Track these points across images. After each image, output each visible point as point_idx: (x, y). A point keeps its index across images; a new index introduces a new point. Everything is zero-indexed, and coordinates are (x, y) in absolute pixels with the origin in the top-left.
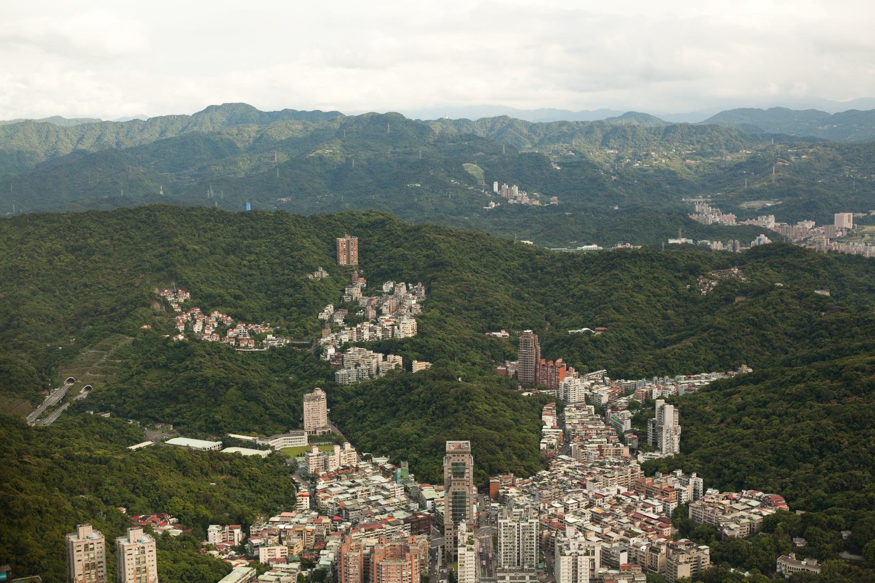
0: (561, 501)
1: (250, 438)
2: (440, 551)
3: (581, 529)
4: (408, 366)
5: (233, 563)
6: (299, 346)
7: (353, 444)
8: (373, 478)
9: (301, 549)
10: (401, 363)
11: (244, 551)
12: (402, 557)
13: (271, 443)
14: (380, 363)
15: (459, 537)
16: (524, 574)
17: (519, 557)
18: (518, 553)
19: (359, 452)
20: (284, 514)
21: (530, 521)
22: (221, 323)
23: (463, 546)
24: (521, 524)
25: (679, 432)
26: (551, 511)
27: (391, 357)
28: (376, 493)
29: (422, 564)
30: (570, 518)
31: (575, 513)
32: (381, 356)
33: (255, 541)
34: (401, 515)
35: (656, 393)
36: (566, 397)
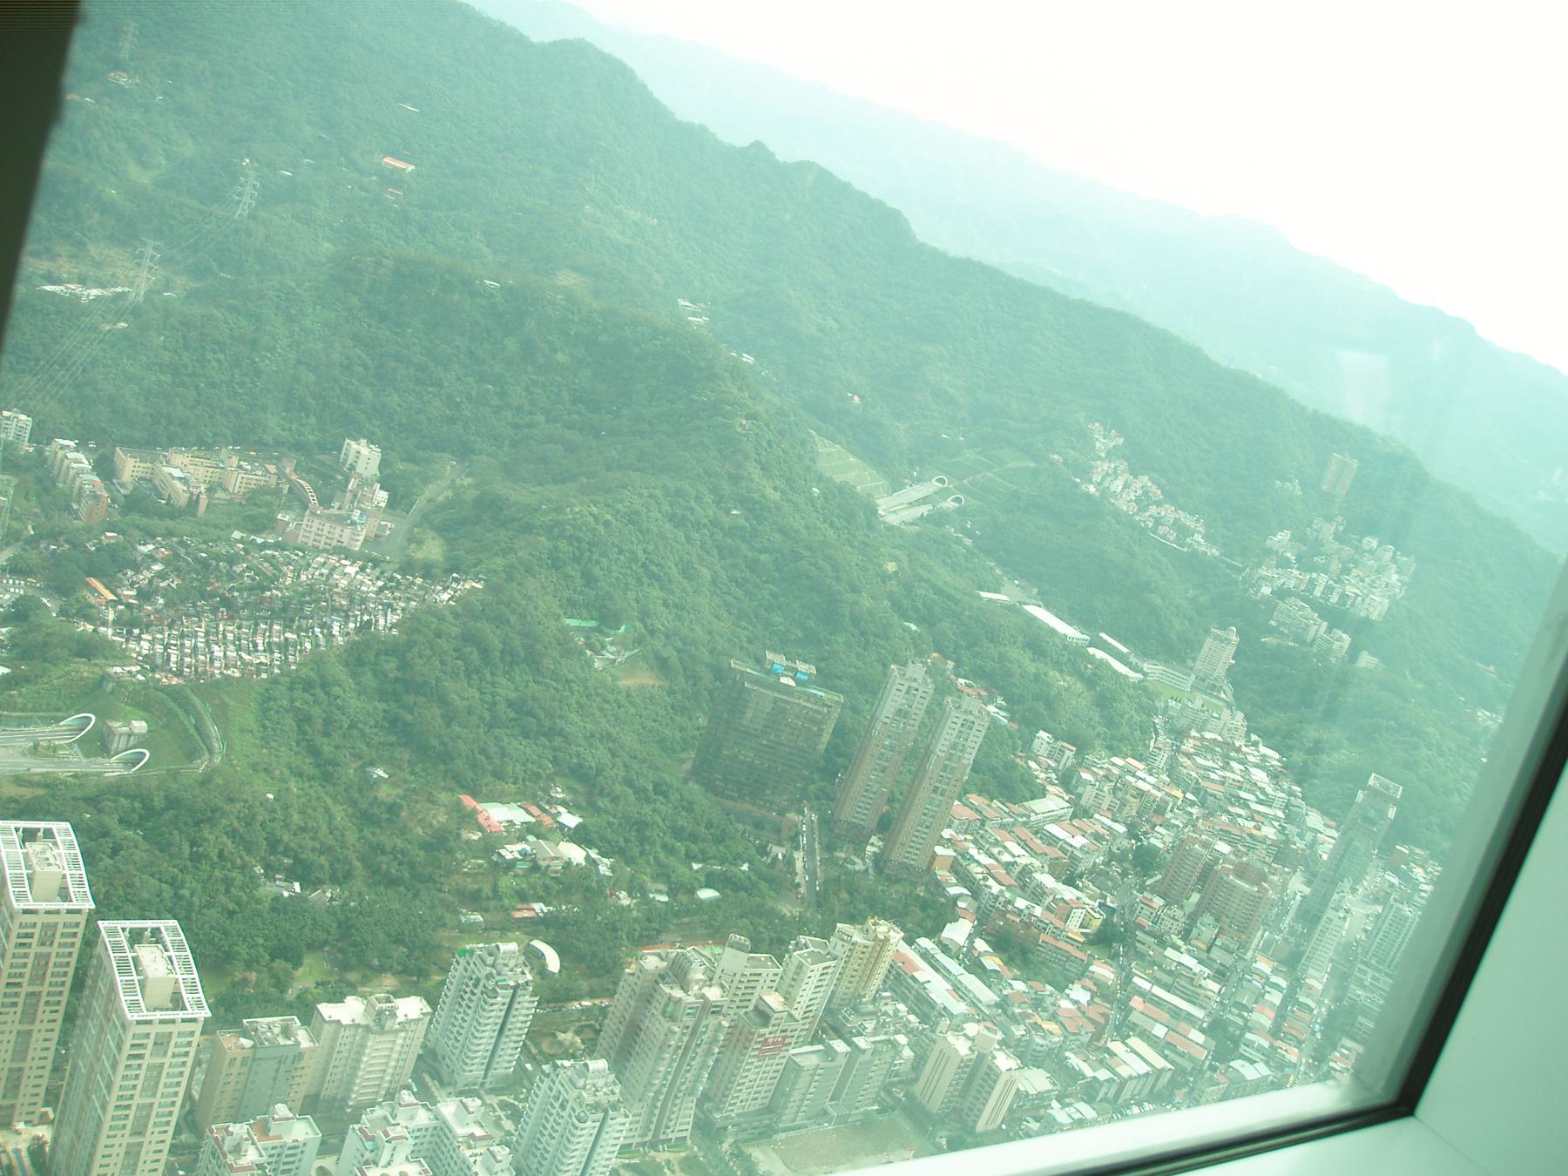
1: (1125, 650)
2: (1298, 898)
5: (1050, 788)
6: (1229, 566)
7: (1247, 718)
8: (1253, 770)
10: (1346, 645)
11: (1067, 780)
13: (1146, 666)
15: (1336, 896)
20: (1130, 760)
22: (1146, 493)
28: (1249, 791)
32: (1325, 624)
33: (1086, 776)
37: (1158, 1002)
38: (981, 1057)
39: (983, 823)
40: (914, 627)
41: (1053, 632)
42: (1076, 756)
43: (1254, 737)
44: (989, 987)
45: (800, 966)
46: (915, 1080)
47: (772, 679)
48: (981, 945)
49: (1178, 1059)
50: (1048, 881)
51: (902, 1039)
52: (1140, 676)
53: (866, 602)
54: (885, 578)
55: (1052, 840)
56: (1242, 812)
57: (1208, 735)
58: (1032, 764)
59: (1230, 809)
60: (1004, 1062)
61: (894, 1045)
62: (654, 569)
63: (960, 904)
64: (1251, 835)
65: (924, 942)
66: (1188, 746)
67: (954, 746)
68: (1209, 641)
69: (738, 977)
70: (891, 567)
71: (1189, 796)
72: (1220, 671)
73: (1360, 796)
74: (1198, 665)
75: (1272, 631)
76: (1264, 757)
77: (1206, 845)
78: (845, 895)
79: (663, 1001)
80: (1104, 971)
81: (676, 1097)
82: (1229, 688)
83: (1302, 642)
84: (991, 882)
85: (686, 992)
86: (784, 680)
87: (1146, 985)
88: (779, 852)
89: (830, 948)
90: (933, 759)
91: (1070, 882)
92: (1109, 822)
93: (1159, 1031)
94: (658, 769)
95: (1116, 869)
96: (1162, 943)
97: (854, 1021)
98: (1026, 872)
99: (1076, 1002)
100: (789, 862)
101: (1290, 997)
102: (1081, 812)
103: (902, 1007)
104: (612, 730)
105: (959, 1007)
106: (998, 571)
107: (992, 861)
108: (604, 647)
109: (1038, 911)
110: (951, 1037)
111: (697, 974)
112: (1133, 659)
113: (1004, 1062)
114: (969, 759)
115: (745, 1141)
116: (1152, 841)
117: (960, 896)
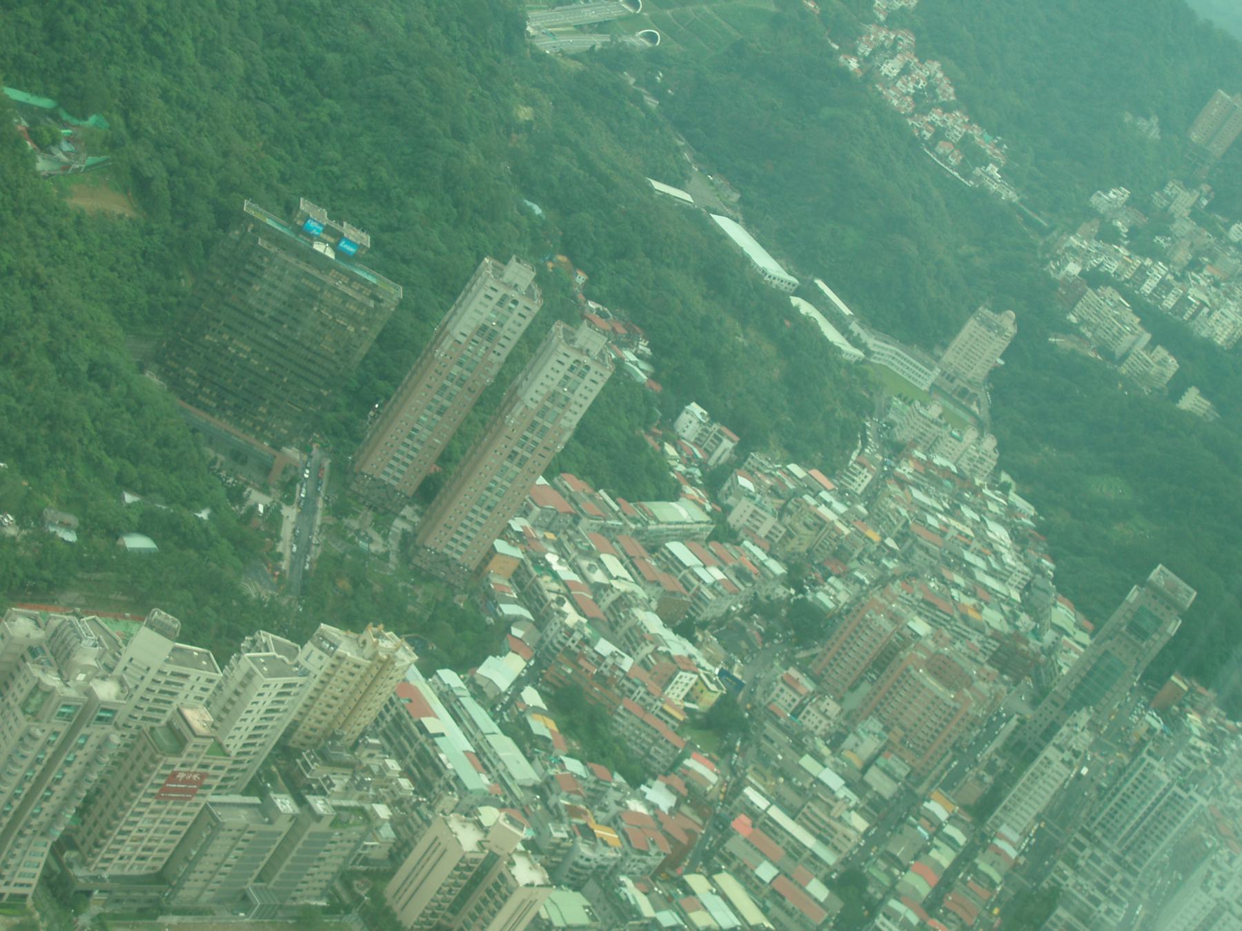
1: (846, 311)
2: (1014, 722)
4: (1177, 388)
6: (1029, 222)
7: (1001, 447)
8: (992, 525)
10: (1170, 373)
13: (871, 342)
14: (1138, 348)
15: (1064, 729)
16: (1117, 867)
19: (1001, 466)
20: (815, 473)
22: (931, 88)
23: (1060, 748)
27: (1161, 352)
28: (979, 553)
32: (1147, 337)
33: (744, 482)
34: (993, 617)
37: (772, 829)
38: (493, 858)
39: (576, 519)
40: (538, 210)
41: (745, 260)
42: (736, 450)
43: (1005, 477)
44: (530, 760)
45: (250, 676)
46: (390, 875)
47: (302, 241)
48: (531, 696)
49: (782, 917)
50: (652, 623)
51: (383, 811)
52: (859, 353)
53: (473, 157)
54: (510, 127)
55: (674, 564)
56: (958, 579)
57: (938, 460)
58: (670, 450)
59: (946, 573)
60: (525, 872)
61: (368, 818)
62: (159, 39)
63: (517, 632)
64: (965, 618)
65: (449, 677)
66: (906, 469)
67: (553, 396)
68: (971, 325)
69: (152, 674)
70: (524, 113)
71: (890, 542)
72: (979, 371)
73: (1133, 595)
74: (949, 356)
75: (1068, 329)
76: (1011, 508)
77: (894, 618)
78: (345, 584)
79: (27, 688)
80: (701, 768)
81: (21, 834)
82: (985, 397)
83: (1108, 355)
84: (567, 607)
85: (65, 682)
86: (319, 247)
87: (760, 802)
88: (261, 502)
89: (301, 657)
90: (518, 410)
91: (685, 630)
92: (762, 556)
93: (766, 872)
94: (102, 341)
95: (757, 625)
96: (799, 747)
97: (318, 771)
98: (623, 602)
99: (652, 806)
100: (274, 519)
101: (965, 858)
102: (723, 532)
103: (393, 765)
104: (41, 270)
105: (477, 781)
106: (686, 156)
107: (575, 578)
108: (55, 141)
109: (627, 663)
110: (455, 823)
111: (87, 655)
112: (855, 327)
113: (525, 872)
114: (571, 420)
115: (115, 917)
116: (821, 596)
117: (516, 620)
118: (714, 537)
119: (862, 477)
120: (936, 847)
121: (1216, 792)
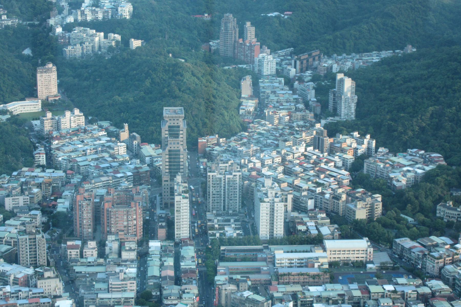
0: (258, 158)
2: (158, 198)
3: (276, 180)
7: (81, 111)
9: (40, 198)
12: (129, 205)
15: (176, 187)
16: (229, 218)
17: (224, 203)
18: (224, 201)
21: (234, 174)
24: (227, 176)
25: (356, 101)
26: (251, 165)
27: (112, 35)
28: (102, 151)
29: (145, 210)
30: (265, 171)
31: (270, 167)
32: (102, 34)
35: (335, 66)
36: (260, 71)
72: (54, 90)
118: (5, 219)
119: (41, 157)
120: (165, 261)
121: (242, 167)
